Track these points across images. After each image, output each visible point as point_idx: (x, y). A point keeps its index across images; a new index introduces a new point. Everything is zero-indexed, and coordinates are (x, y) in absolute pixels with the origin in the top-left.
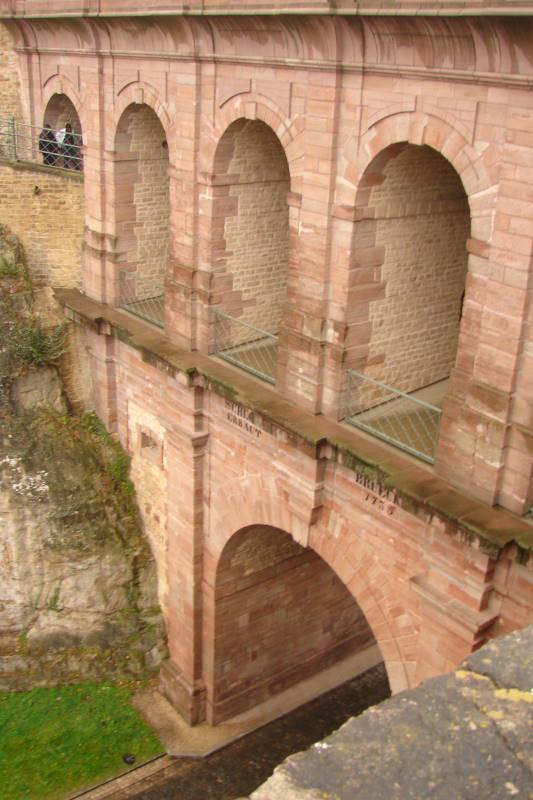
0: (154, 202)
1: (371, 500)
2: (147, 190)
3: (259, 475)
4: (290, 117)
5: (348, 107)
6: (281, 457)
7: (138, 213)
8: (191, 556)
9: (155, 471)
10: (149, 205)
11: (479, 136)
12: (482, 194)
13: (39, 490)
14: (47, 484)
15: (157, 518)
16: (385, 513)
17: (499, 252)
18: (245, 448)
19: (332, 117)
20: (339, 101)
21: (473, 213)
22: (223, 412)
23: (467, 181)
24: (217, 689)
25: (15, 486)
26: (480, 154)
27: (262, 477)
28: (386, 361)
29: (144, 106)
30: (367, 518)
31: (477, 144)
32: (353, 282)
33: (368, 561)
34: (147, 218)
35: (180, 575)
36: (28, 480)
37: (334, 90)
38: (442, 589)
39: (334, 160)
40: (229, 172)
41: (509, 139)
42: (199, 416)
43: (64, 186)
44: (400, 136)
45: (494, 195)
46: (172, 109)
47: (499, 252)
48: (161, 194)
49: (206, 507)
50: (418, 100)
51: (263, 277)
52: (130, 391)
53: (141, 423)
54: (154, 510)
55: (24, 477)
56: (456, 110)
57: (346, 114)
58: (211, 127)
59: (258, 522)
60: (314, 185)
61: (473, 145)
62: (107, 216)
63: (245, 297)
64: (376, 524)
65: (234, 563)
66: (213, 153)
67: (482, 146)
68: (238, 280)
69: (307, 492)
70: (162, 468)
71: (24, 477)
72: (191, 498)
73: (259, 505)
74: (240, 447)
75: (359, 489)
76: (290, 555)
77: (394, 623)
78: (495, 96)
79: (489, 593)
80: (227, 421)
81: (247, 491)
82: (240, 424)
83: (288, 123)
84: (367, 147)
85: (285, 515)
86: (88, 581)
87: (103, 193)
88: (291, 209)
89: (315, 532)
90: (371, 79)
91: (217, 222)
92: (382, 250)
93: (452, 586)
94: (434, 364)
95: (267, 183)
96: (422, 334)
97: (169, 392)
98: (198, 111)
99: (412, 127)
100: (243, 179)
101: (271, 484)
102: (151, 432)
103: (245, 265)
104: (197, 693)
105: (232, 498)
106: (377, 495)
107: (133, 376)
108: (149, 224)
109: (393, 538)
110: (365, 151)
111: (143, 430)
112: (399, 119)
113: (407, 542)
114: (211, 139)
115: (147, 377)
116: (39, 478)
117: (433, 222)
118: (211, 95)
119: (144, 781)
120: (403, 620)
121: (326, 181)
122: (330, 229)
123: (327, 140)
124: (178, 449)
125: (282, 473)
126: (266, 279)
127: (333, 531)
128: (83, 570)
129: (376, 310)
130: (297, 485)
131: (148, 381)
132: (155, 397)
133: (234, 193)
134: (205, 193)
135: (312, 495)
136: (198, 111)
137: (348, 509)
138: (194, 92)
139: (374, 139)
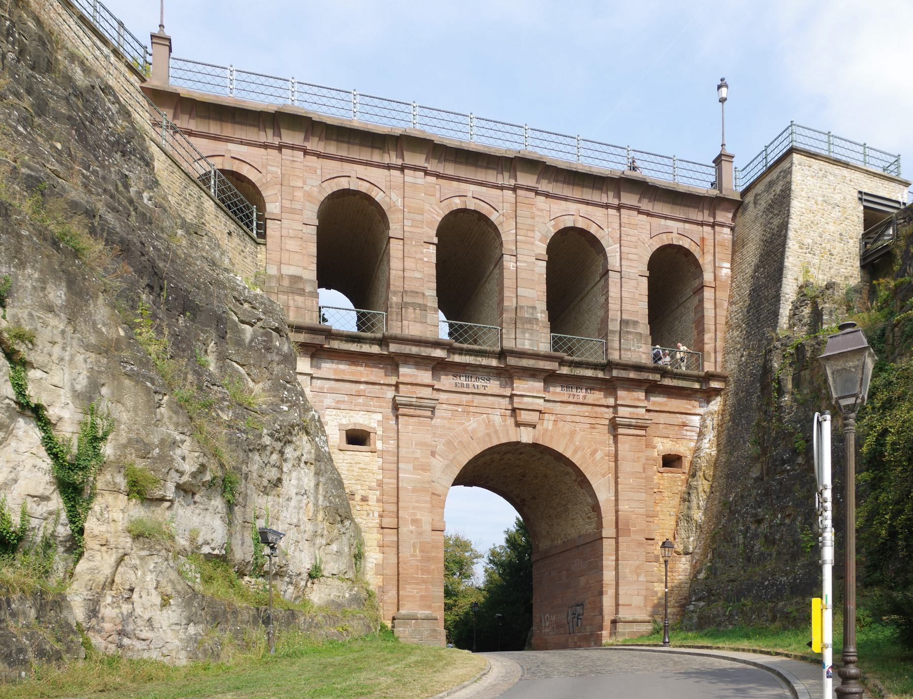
15: (364, 499)
30: (571, 407)
35: (415, 522)
73: (488, 435)
75: (564, 394)
81: (474, 431)
120: (599, 455)
127: (548, 426)
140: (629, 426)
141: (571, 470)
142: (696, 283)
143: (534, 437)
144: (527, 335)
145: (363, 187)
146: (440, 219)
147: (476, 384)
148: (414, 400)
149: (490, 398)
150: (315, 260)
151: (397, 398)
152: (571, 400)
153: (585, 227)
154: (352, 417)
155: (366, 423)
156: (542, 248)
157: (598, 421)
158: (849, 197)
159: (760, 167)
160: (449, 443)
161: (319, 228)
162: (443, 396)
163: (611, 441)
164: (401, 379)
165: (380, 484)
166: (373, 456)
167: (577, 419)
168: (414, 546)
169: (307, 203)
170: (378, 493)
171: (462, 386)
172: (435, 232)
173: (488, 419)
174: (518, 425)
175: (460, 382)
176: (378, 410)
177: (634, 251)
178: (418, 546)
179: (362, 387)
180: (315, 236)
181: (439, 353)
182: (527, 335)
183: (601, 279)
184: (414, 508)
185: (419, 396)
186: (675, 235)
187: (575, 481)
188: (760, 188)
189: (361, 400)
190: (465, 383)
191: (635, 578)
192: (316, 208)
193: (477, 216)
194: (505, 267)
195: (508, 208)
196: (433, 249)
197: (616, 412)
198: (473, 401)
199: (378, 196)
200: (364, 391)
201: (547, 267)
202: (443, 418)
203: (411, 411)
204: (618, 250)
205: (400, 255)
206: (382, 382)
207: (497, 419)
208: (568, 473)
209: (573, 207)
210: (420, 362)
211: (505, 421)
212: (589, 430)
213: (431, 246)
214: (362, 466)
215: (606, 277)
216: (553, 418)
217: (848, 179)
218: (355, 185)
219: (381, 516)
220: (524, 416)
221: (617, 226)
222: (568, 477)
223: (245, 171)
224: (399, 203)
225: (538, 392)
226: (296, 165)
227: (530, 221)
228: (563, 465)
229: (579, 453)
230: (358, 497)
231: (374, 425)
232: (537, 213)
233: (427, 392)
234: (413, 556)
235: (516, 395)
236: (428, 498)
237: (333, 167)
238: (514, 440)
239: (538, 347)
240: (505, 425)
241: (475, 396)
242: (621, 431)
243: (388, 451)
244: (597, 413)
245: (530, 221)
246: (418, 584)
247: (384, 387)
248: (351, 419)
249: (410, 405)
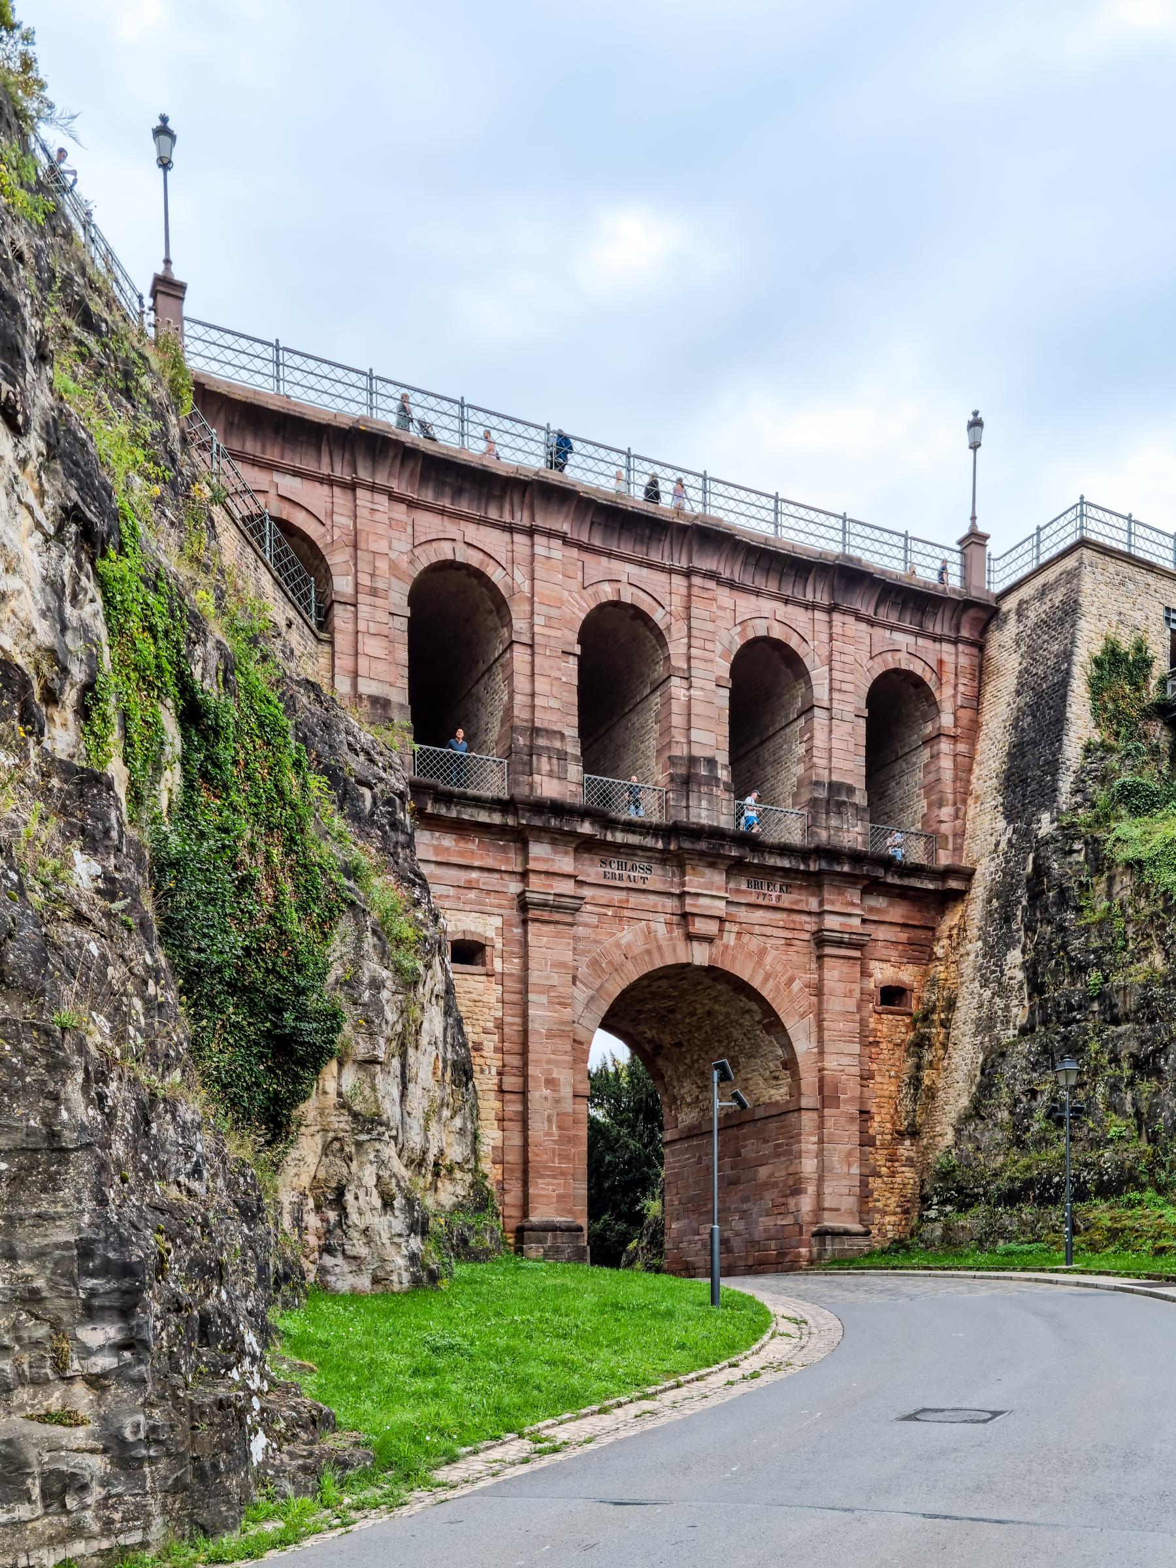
1: (761, 898)
15: (478, 1047)
22: (597, 873)
35: (551, 1083)
44: (762, 633)
73: (649, 952)
81: (628, 945)
85: (681, 945)
112: (757, 621)
120: (797, 985)
140: (839, 943)
141: (754, 1007)
142: (929, 729)
143: (710, 958)
144: (704, 803)
145: (474, 559)
146: (583, 616)
147: (632, 874)
148: (551, 898)
149: (652, 897)
150: (406, 672)
151: (528, 894)
152: (760, 901)
153: (782, 638)
154: (460, 920)
155: (480, 930)
156: (723, 668)
157: (797, 935)
158: (1152, 616)
159: (1027, 558)
160: (594, 963)
161: (410, 620)
162: (587, 892)
163: (814, 966)
164: (532, 865)
165: (500, 1025)
166: (490, 982)
167: (769, 931)
168: (549, 1120)
169: (394, 580)
170: (496, 1037)
171: (614, 876)
172: (576, 636)
173: (649, 928)
174: (690, 937)
176: (496, 911)
177: (849, 677)
178: (554, 1119)
179: (474, 875)
180: (406, 634)
181: (586, 828)
183: (799, 717)
184: (549, 1062)
185: (558, 891)
186: (903, 656)
187: (759, 1022)
188: (1026, 592)
189: (472, 895)
190: (617, 872)
191: (845, 1169)
192: (407, 588)
193: (632, 611)
195: (677, 603)
196: (573, 664)
197: (821, 922)
198: (627, 901)
199: (496, 575)
201: (730, 698)
202: (586, 925)
203: (546, 916)
204: (827, 675)
205: (527, 669)
206: (503, 868)
207: (661, 929)
208: (749, 1011)
209: (767, 606)
210: (559, 838)
211: (670, 931)
212: (784, 948)
213: (571, 657)
214: (474, 996)
215: (810, 715)
216: (735, 928)
217: (1153, 588)
218: (464, 556)
219: (500, 1074)
220: (700, 926)
221: (825, 637)
222: (747, 1016)
223: (299, 519)
224: (526, 588)
225: (719, 889)
226: (378, 517)
227: (709, 626)
228: (744, 999)
229: (771, 983)
232: (720, 613)
233: (567, 887)
234: (548, 1134)
235: (689, 893)
236: (568, 1048)
237: (430, 524)
238: (683, 960)
239: (719, 821)
240: (671, 939)
241: (633, 895)
242: (828, 950)
243: (511, 975)
244: (794, 922)
245: (709, 626)
246: (554, 1177)
247: (506, 876)
248: (459, 924)
249: (544, 905)
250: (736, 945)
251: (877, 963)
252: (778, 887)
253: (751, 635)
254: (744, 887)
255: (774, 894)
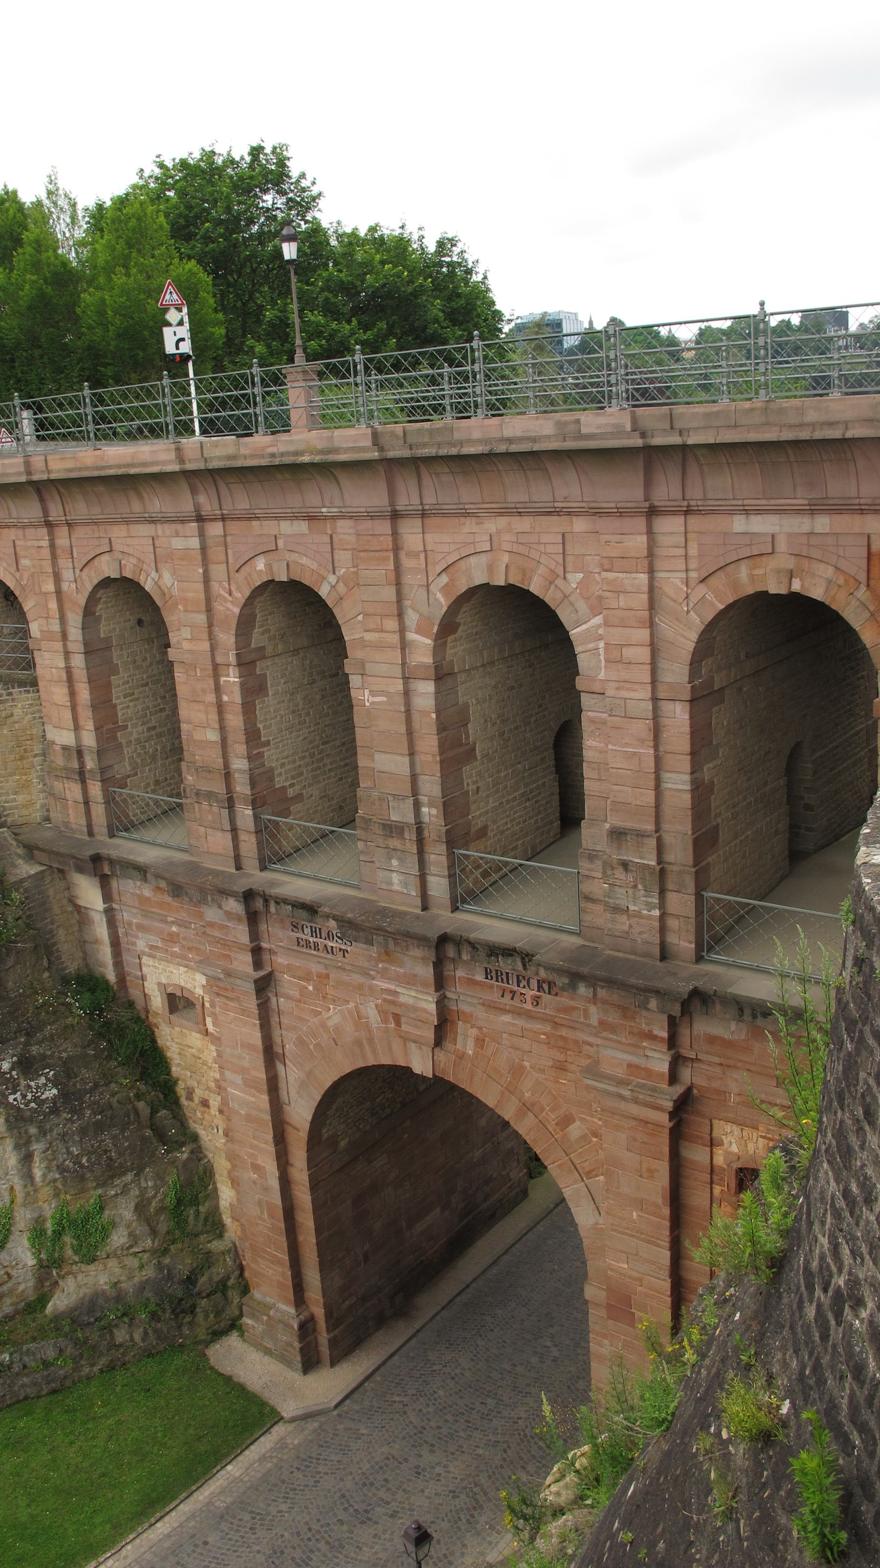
0: (136, 696)
1: (508, 996)
2: (128, 682)
3: (351, 1005)
4: (334, 573)
5: (408, 554)
6: (384, 974)
7: (120, 714)
8: (270, 1137)
9: (195, 1039)
10: (132, 701)
11: (570, 567)
12: (584, 627)
13: (44, 1097)
14: (55, 1086)
15: (205, 1103)
16: (528, 1006)
17: (615, 685)
18: (327, 976)
19: (392, 567)
20: (396, 549)
21: (578, 649)
23: (565, 616)
24: (329, 1315)
25: (11, 1098)
26: (574, 586)
27: (356, 1007)
28: (491, 834)
29: (125, 580)
30: (507, 1018)
31: (569, 576)
32: (443, 748)
33: (517, 1071)
34: (131, 719)
35: (256, 1168)
36: (29, 1087)
37: (390, 538)
38: (620, 1072)
39: (400, 615)
40: (253, 646)
41: (606, 567)
42: (257, 952)
43: (10, 694)
45: (599, 626)
46: (167, 579)
47: (615, 685)
48: (143, 686)
49: (280, 1067)
50: (494, 538)
51: (307, 765)
52: (141, 944)
53: (164, 981)
54: (199, 1093)
55: (23, 1083)
56: (539, 543)
57: (407, 563)
58: (227, 595)
59: (361, 1064)
60: (379, 646)
61: (565, 578)
62: (82, 722)
63: (291, 793)
64: (521, 1022)
65: (326, 1133)
66: (234, 626)
67: (575, 578)
68: (280, 774)
69: (424, 1005)
70: (207, 1033)
71: (23, 1083)
72: (259, 1060)
73: (358, 1043)
74: (319, 976)
75: (491, 987)
76: (388, 1111)
77: (565, 1135)
78: (580, 525)
79: (677, 1062)
80: (296, 948)
81: (337, 1029)
82: (316, 947)
83: (332, 579)
84: (439, 596)
85: (397, 1044)
86: (125, 1210)
87: (72, 694)
88: (351, 677)
89: (441, 1056)
90: (431, 521)
91: (248, 709)
92: (466, 706)
93: (629, 1065)
94: (538, 828)
95: (296, 651)
96: (522, 795)
97: (209, 931)
98: (207, 579)
99: (491, 568)
100: (269, 651)
101: (371, 1013)
102: (182, 988)
103: (286, 753)
104: (302, 1326)
105: (318, 1046)
106: (515, 988)
107: (146, 922)
108: (135, 726)
109: (544, 1034)
110: (437, 600)
111: (170, 990)
112: (473, 560)
113: (564, 1032)
114: (229, 609)
115: (170, 919)
116: (43, 1080)
117: (511, 666)
118: (222, 557)
119: (263, 1458)
120: (575, 1130)
121: (395, 638)
122: (407, 693)
123: (389, 593)
124: (231, 999)
125: (388, 991)
126: (309, 768)
127: (465, 1046)
128: (116, 1195)
129: (470, 774)
130: (411, 1001)
131: (173, 923)
132: (184, 943)
133: (262, 669)
134: (228, 676)
135: (432, 1007)
136: (207, 579)
137: (480, 1013)
138: (199, 558)
139: (447, 585)
175: (304, 937)
182: (395, 862)
184: (252, 1146)
190: (311, 939)
194: (354, 702)
200: (178, 935)
202: (288, 997)
211: (385, 1021)
216: (474, 1031)
230: (196, 1100)
231: (199, 991)
250: (476, 1054)
251: (728, 1127)
252: (533, 983)
253: (463, 586)
254: (480, 977)
255: (530, 993)
